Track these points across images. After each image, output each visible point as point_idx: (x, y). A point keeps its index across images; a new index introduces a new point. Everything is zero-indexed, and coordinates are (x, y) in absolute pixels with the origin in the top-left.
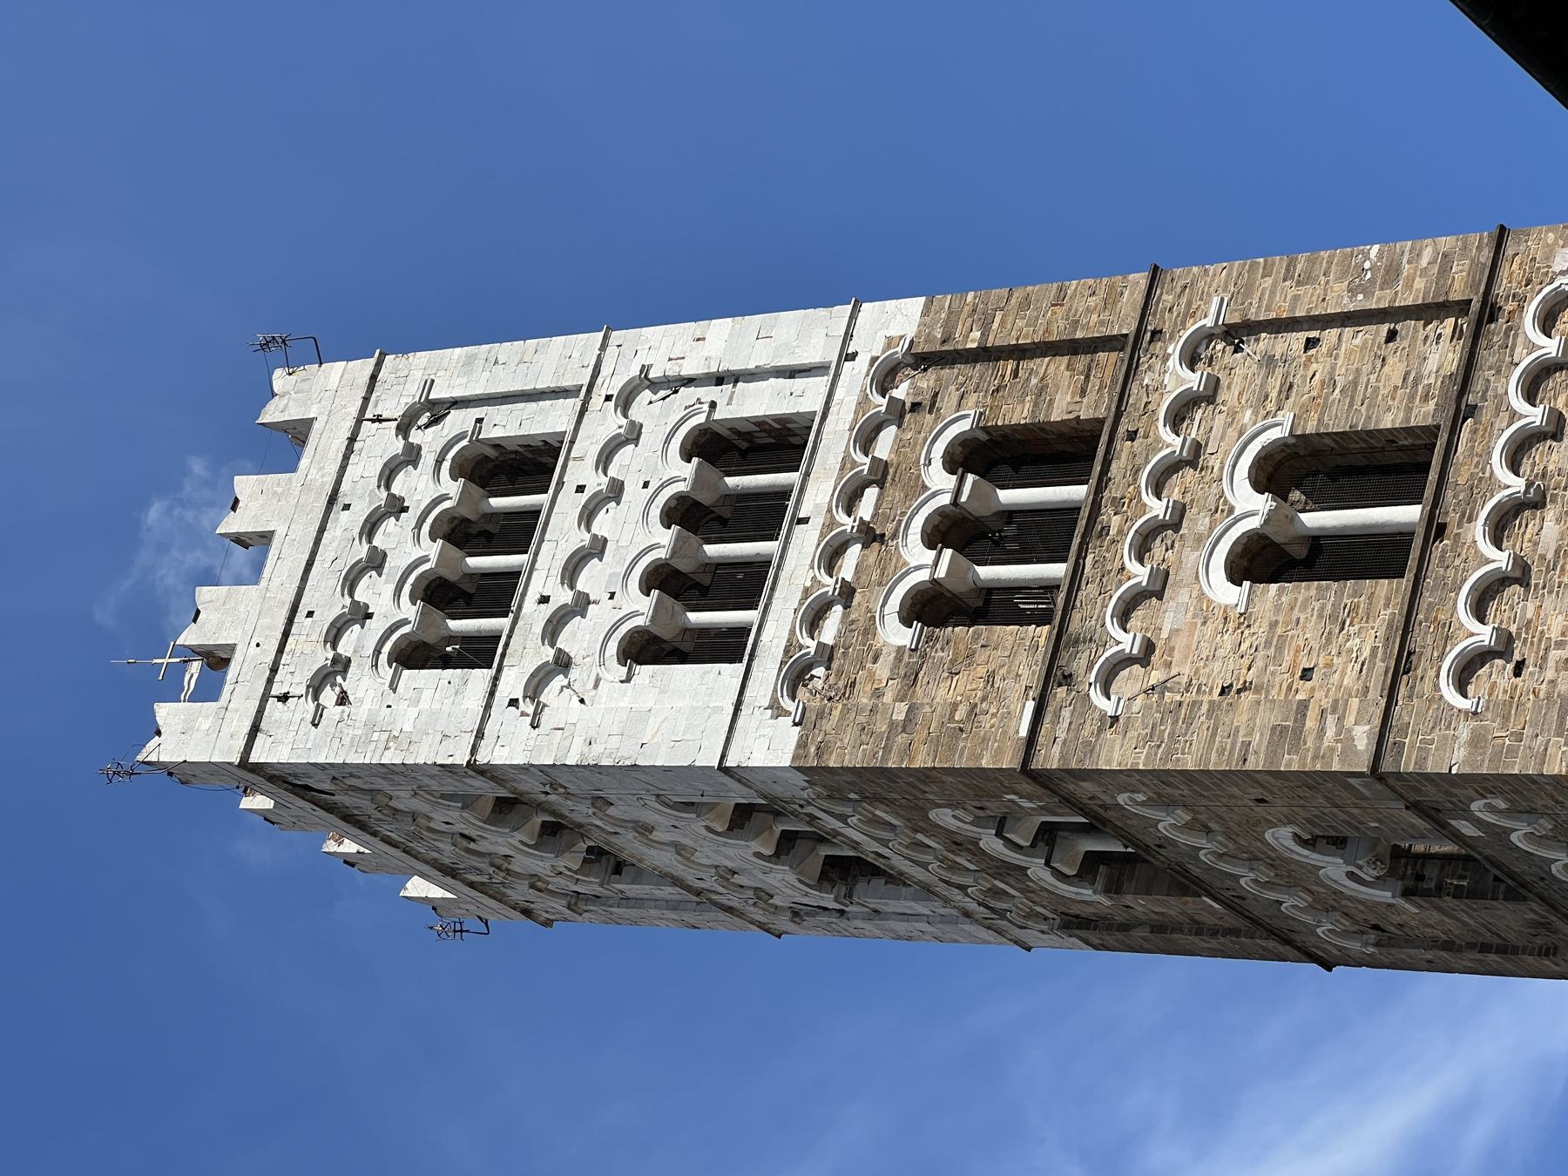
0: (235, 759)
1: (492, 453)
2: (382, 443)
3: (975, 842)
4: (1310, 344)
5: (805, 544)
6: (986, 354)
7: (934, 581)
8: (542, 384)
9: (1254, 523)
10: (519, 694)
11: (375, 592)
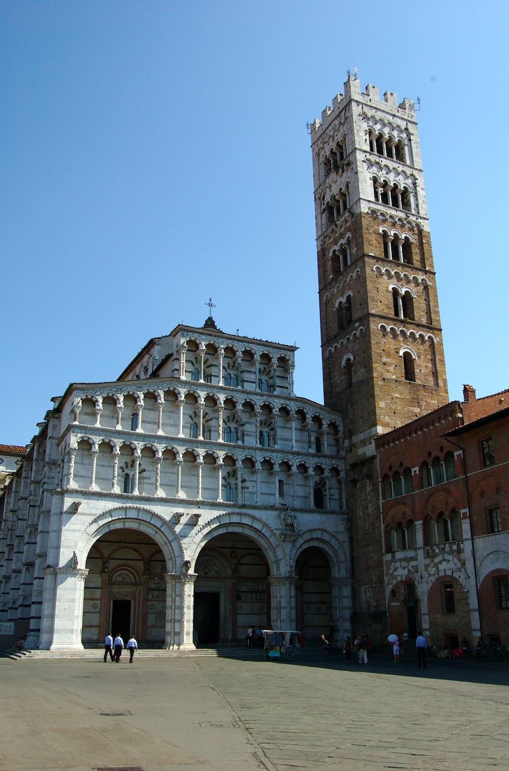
0: (352, 97)
1: (402, 146)
2: (403, 125)
5: (393, 212)
6: (421, 244)
8: (415, 159)
10: (367, 157)
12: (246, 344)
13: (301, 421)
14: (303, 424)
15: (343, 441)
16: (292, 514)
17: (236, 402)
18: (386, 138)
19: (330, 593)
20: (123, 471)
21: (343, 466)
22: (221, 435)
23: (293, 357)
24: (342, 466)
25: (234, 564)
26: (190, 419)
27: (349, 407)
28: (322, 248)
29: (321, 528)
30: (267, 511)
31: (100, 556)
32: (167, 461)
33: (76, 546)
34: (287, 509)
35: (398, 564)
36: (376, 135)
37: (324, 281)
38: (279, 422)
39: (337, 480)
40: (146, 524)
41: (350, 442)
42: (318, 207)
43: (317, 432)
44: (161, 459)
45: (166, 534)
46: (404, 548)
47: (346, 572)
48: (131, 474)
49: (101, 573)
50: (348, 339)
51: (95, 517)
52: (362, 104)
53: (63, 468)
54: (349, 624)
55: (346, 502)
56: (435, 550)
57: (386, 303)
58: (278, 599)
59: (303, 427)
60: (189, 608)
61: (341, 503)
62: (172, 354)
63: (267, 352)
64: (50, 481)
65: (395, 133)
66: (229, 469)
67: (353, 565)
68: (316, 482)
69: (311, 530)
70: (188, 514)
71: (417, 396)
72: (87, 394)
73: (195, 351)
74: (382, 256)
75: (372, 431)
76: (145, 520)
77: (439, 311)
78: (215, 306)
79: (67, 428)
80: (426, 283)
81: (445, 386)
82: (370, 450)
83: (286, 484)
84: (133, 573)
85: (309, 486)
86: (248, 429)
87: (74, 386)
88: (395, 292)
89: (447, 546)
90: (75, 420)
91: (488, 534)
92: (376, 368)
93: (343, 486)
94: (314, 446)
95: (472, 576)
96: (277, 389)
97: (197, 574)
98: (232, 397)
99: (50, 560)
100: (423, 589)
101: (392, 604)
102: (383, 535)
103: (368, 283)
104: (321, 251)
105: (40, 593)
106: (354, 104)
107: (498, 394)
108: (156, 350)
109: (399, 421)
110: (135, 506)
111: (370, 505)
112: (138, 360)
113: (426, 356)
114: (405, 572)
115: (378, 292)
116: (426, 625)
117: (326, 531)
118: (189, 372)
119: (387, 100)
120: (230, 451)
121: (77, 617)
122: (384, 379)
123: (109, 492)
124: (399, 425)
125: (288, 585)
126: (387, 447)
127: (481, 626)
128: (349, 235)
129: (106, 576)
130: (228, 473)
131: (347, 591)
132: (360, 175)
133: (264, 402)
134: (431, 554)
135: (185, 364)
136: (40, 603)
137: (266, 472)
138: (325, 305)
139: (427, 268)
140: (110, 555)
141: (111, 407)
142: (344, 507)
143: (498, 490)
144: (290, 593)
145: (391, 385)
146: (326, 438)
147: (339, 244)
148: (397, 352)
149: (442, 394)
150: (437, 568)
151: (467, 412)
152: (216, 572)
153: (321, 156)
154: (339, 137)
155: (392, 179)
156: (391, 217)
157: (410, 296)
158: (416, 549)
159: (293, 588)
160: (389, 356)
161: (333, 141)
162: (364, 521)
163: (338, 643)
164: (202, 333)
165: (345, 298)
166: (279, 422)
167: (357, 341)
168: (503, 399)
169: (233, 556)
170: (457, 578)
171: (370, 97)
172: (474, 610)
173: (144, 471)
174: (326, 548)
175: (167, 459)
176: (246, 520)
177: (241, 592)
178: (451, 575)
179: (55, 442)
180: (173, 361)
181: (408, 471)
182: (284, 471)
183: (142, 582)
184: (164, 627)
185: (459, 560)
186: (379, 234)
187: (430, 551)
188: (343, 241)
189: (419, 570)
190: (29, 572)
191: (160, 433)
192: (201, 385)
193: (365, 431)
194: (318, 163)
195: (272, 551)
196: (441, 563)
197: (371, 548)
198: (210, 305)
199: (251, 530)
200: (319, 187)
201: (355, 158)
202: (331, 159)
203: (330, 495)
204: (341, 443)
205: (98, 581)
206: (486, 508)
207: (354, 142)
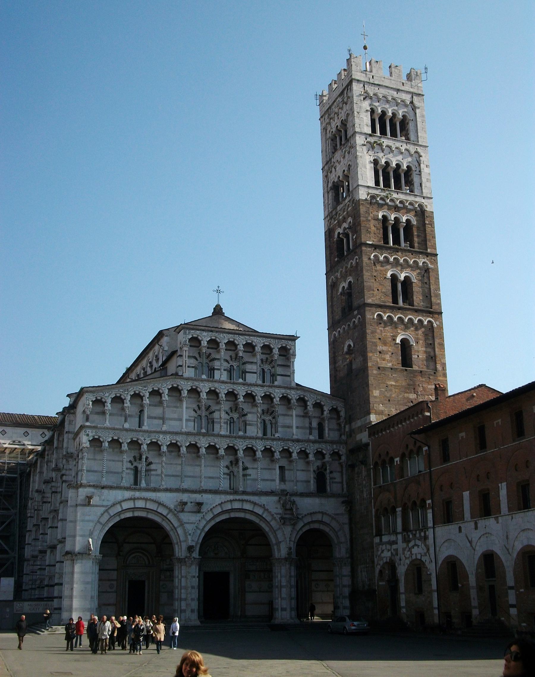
0: (353, 77)
1: (407, 122)
4: (426, 283)
7: (389, 220)
8: (419, 134)
12: (247, 337)
13: (304, 408)
14: (305, 411)
15: (345, 427)
16: (293, 498)
17: (237, 395)
18: (390, 116)
19: (332, 571)
20: (132, 464)
21: (344, 451)
26: (194, 412)
28: (329, 229)
30: (267, 497)
32: (173, 454)
34: (287, 494)
35: (384, 547)
36: (378, 114)
37: (330, 263)
38: (280, 410)
39: (339, 464)
40: (153, 512)
42: (326, 185)
43: (319, 417)
45: (172, 521)
50: (349, 325)
51: (106, 508)
52: (364, 82)
53: (78, 462)
54: (348, 601)
55: (346, 485)
57: (383, 290)
58: (279, 579)
59: (304, 413)
61: (343, 486)
62: (177, 351)
63: (268, 344)
64: (67, 472)
66: (232, 458)
69: (311, 514)
71: (413, 382)
72: (97, 396)
73: (199, 347)
75: (366, 420)
76: (152, 509)
79: (80, 427)
80: (427, 266)
81: (444, 370)
82: (364, 437)
83: (288, 470)
85: (310, 471)
86: (250, 419)
88: (394, 278)
89: (418, 532)
91: (445, 524)
93: (344, 469)
94: (316, 433)
96: (279, 378)
98: (234, 390)
100: (401, 570)
101: (380, 583)
102: (374, 519)
103: (364, 272)
104: (328, 232)
105: (61, 576)
108: (165, 340)
109: (393, 408)
111: (365, 490)
114: (389, 554)
116: (403, 604)
117: (326, 514)
118: (193, 367)
120: (232, 442)
122: (379, 368)
124: (394, 412)
125: (288, 566)
128: (350, 220)
130: (231, 462)
131: (346, 570)
132: (360, 161)
133: (265, 393)
136: (61, 584)
137: (268, 459)
138: (331, 287)
139: (429, 250)
141: (120, 406)
142: (345, 490)
143: (451, 485)
144: (290, 573)
145: (387, 373)
146: (326, 425)
147: (343, 227)
149: (441, 378)
150: (411, 552)
151: (436, 410)
153: (328, 131)
154: (343, 116)
158: (395, 533)
159: (293, 568)
160: (385, 344)
161: (338, 118)
164: (203, 330)
165: (347, 283)
168: (475, 394)
170: (424, 561)
171: (372, 74)
172: (434, 591)
173: (151, 463)
174: (327, 529)
175: (172, 452)
176: (247, 506)
178: (420, 558)
179: (71, 436)
180: (178, 357)
181: (392, 460)
182: (286, 457)
184: (172, 605)
185: (425, 545)
186: (377, 219)
187: (406, 536)
188: (345, 225)
190: (53, 555)
193: (362, 418)
195: (272, 533)
196: (414, 548)
198: (218, 291)
199: (252, 514)
200: (326, 164)
202: (337, 136)
203: (331, 478)
204: (343, 427)
205: (113, 563)
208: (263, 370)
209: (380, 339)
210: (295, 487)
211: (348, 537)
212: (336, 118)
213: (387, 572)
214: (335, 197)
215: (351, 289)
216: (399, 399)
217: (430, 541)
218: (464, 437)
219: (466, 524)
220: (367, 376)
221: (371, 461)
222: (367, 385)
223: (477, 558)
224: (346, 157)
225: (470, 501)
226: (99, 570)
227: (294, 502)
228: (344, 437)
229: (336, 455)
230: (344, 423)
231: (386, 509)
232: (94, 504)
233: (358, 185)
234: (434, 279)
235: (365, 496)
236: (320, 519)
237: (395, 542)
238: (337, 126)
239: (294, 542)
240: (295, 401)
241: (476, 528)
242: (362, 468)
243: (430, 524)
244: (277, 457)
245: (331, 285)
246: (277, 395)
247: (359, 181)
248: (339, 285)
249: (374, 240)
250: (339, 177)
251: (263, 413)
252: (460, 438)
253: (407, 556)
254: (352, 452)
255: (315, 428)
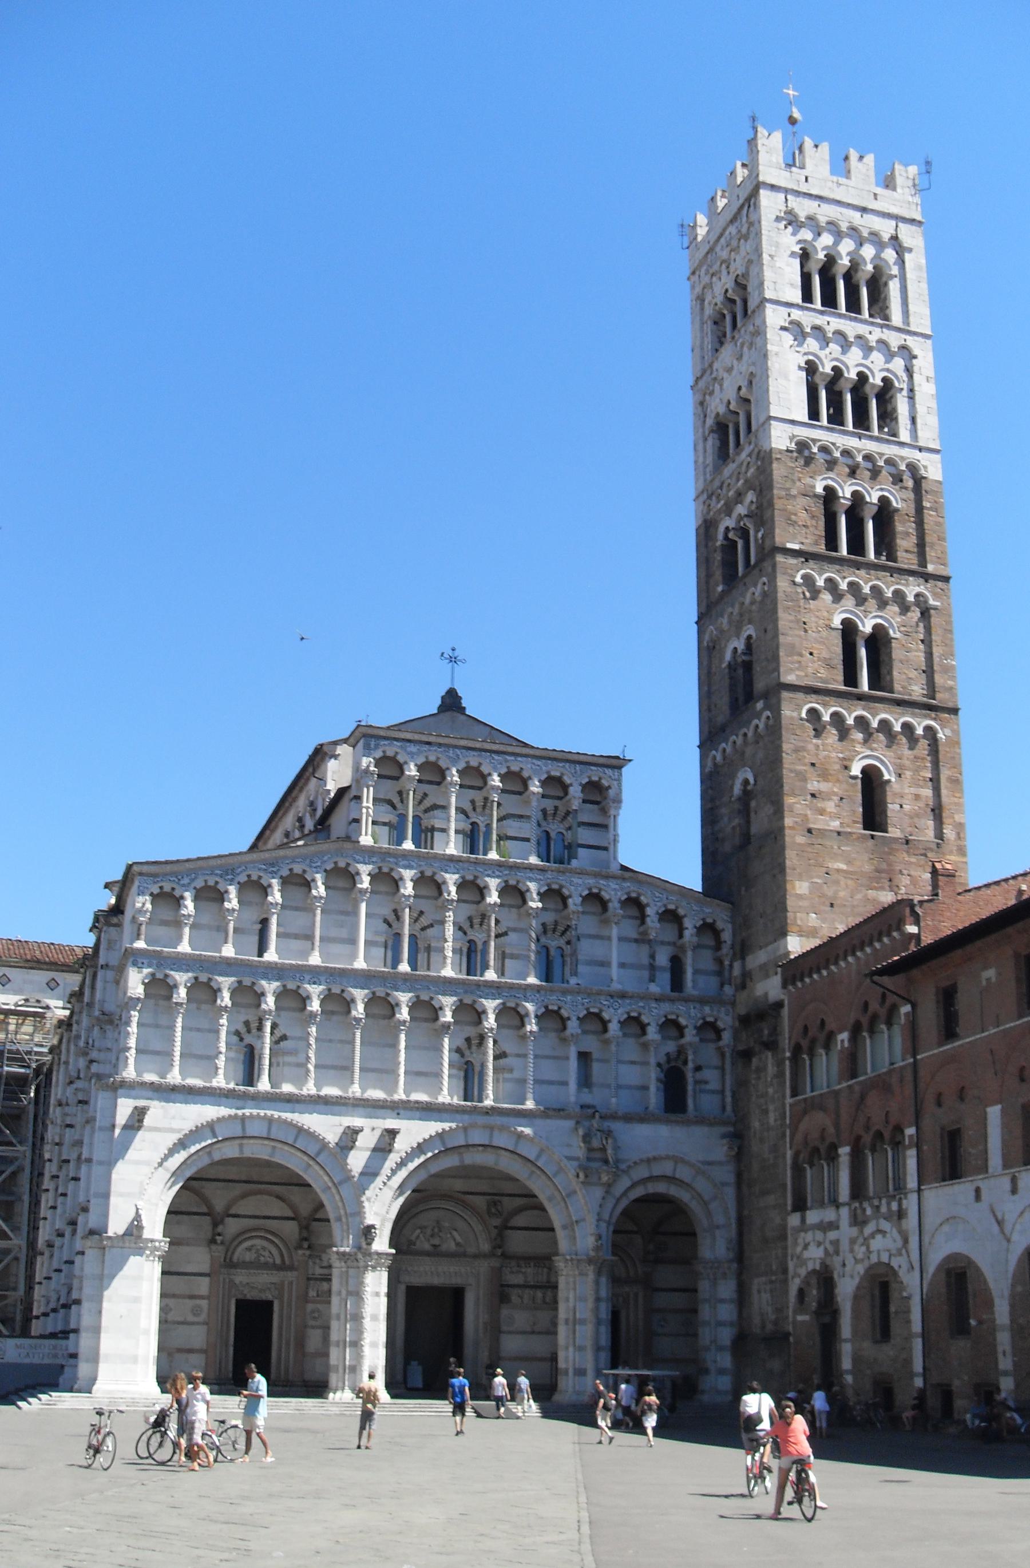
0: (761, 178)
1: (884, 279)
2: (886, 228)
3: (741, 503)
5: (852, 443)
6: (919, 509)
8: (911, 307)
9: (861, 628)
10: (793, 317)
11: (827, 239)
12: (508, 758)
13: (638, 922)
14: (642, 929)
15: (731, 966)
16: (607, 1124)
20: (241, 1039)
22: (449, 961)
23: (619, 780)
24: (726, 1020)
25: (496, 1227)
26: (385, 926)
27: (743, 889)
28: (705, 521)
29: (671, 1154)
31: (204, 1209)
32: (335, 1018)
33: (142, 1193)
34: (593, 1116)
35: (809, 1236)
37: (708, 597)
40: (286, 1148)
41: (743, 966)
43: (674, 944)
44: (316, 1015)
46: (822, 1205)
47: (728, 1249)
48: (257, 1046)
49: (209, 1246)
50: (745, 735)
52: (786, 191)
56: (864, 1210)
59: (641, 934)
60: (375, 1318)
61: (723, 1100)
64: (102, 1056)
65: (868, 252)
66: (471, 1031)
67: (740, 1234)
68: (668, 1054)
70: (373, 1129)
74: (821, 549)
77: (953, 668)
78: (464, 661)
80: (926, 602)
82: (771, 988)
83: (598, 1060)
84: (277, 1246)
87: (135, 868)
88: (849, 630)
89: (884, 1201)
90: (138, 937)
91: (944, 1180)
92: (791, 806)
95: (917, 1265)
96: (582, 852)
97: (393, 1251)
99: (92, 1220)
100: (846, 1288)
101: (800, 1318)
106: (764, 194)
107: (1014, 878)
110: (262, 1113)
111: (771, 1107)
112: (300, 784)
113: (916, 771)
115: (806, 631)
116: (846, 1364)
117: (683, 1161)
118: (385, 824)
119: (849, 172)
121: (147, 1332)
122: (810, 831)
123: (208, 1085)
125: (591, 1276)
126: (799, 984)
127: (924, 1368)
128: (750, 496)
129: (219, 1251)
131: (727, 1289)
132: (773, 364)
134: (860, 1218)
135: (371, 811)
137: (553, 1035)
138: (708, 651)
139: (930, 568)
140: (229, 1207)
141: (213, 906)
142: (729, 1108)
143: (961, 1094)
145: (828, 843)
147: (735, 515)
148: (846, 768)
150: (868, 1248)
152: (458, 1244)
153: (706, 302)
154: (738, 267)
155: (853, 363)
156: (846, 453)
157: (888, 634)
158: (836, 1204)
159: (603, 1280)
160: (825, 776)
161: (728, 273)
162: (762, 1140)
163: (705, 1398)
166: (586, 924)
167: (761, 744)
169: (493, 1210)
170: (896, 1268)
171: (805, 172)
173: (284, 1038)
175: (333, 1013)
177: (508, 1286)
178: (887, 1261)
180: (351, 800)
181: (830, 1037)
183: (296, 1263)
187: (859, 1211)
188: (741, 510)
189: (841, 1249)
191: (315, 959)
192: (406, 855)
193: (767, 945)
194: (701, 320)
197: (771, 1199)
198: (453, 660)
201: (764, 322)
202: (726, 312)
203: (697, 1082)
204: (727, 967)
205: (200, 1259)
206: (942, 1129)
207: (761, 284)
208: (547, 833)
209: (813, 764)
210: (614, 1100)
211: (733, 1214)
212: (724, 272)
213: (815, 1292)
214: (720, 448)
215: (751, 654)
216: (855, 903)
217: (911, 1222)
218: (994, 980)
219: (992, 1181)
220: (783, 848)
221: (786, 1043)
222: (782, 869)
223: (1014, 1258)
224: (745, 358)
225: (1002, 1129)
226: (163, 1273)
227: (608, 1134)
228: (728, 990)
229: (709, 1029)
230: (729, 957)
231: (816, 1150)
232: (152, 1125)
233: (770, 418)
234: (940, 631)
235: (772, 1120)
236: (669, 1173)
237: (833, 1226)
238: (727, 291)
239: (609, 1223)
240: (617, 905)
241: (1014, 1191)
242: (767, 1057)
243: (912, 1182)
244: (574, 1031)
245: (708, 646)
246: (576, 890)
247: (772, 407)
248: (726, 646)
249: (804, 541)
250: (729, 403)
251: (545, 932)
252: (984, 983)
253: (860, 1256)
254: (745, 1021)
255: (662, 969)
